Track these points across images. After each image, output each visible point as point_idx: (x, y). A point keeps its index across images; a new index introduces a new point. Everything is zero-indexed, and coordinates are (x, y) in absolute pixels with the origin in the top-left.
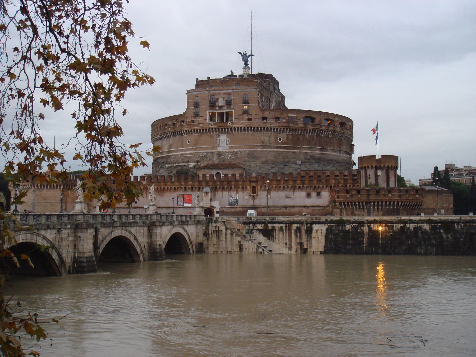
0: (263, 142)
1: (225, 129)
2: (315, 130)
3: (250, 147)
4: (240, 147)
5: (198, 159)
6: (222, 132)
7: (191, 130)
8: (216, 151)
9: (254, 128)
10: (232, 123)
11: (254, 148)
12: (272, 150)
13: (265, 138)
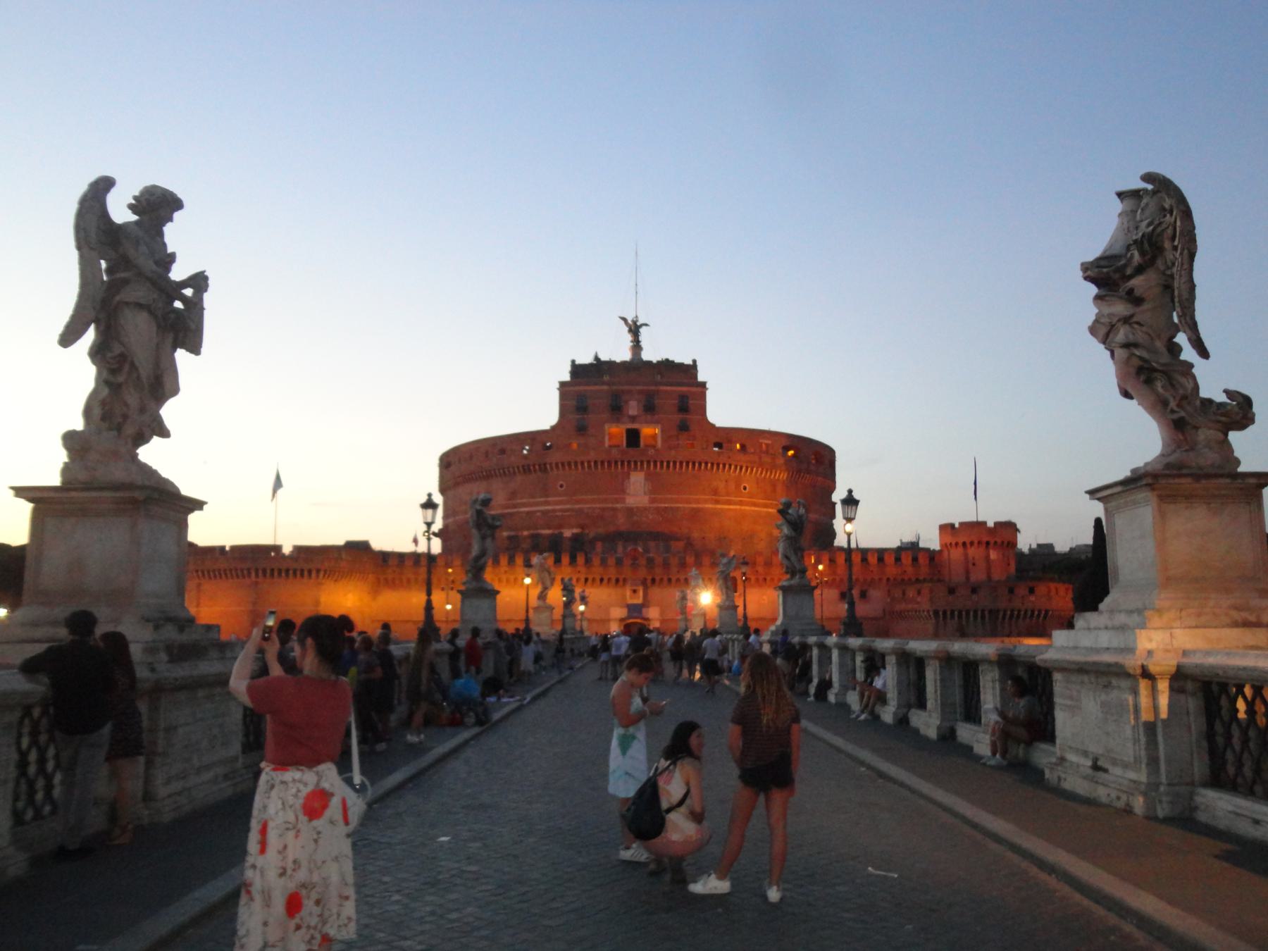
0: (715, 492)
1: (642, 462)
3: (688, 502)
9: (700, 464)
10: (657, 451)
11: (698, 501)
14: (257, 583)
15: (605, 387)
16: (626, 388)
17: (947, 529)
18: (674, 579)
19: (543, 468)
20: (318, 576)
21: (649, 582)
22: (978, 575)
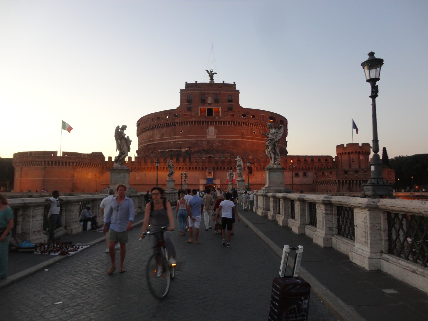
0: (243, 134)
1: (213, 122)
3: (232, 138)
5: (190, 146)
6: (211, 124)
7: (184, 122)
9: (237, 122)
11: (236, 138)
14: (45, 168)
15: (198, 92)
16: (207, 92)
17: (340, 147)
18: (226, 168)
20: (73, 165)
22: (355, 166)
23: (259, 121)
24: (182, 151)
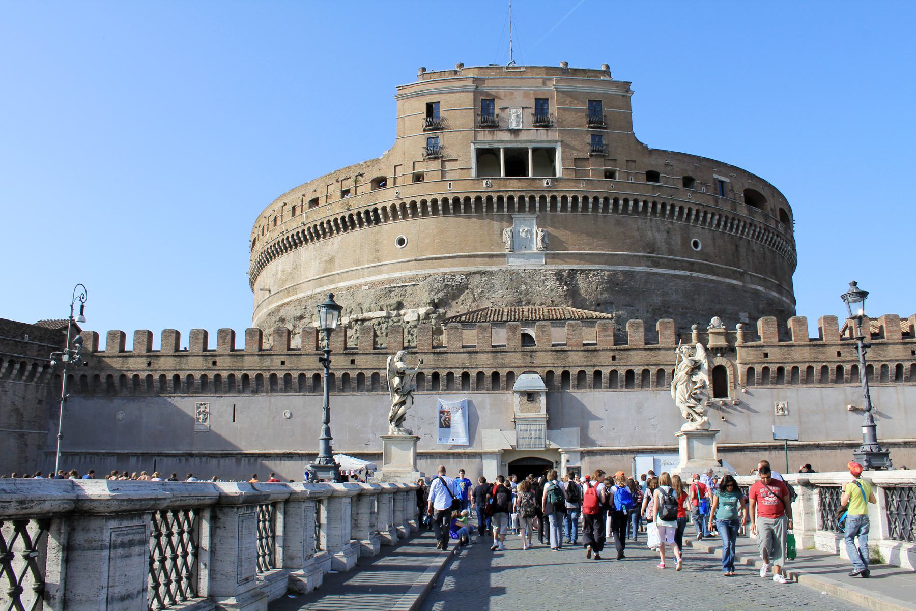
0: (651, 247)
1: (532, 198)
2: (769, 232)
4: (581, 258)
6: (521, 209)
7: (414, 204)
8: (503, 268)
9: (626, 201)
12: (678, 272)
13: (657, 234)
18: (606, 372)
19: (373, 217)
21: (557, 382)
23: (712, 204)
24: (406, 319)
